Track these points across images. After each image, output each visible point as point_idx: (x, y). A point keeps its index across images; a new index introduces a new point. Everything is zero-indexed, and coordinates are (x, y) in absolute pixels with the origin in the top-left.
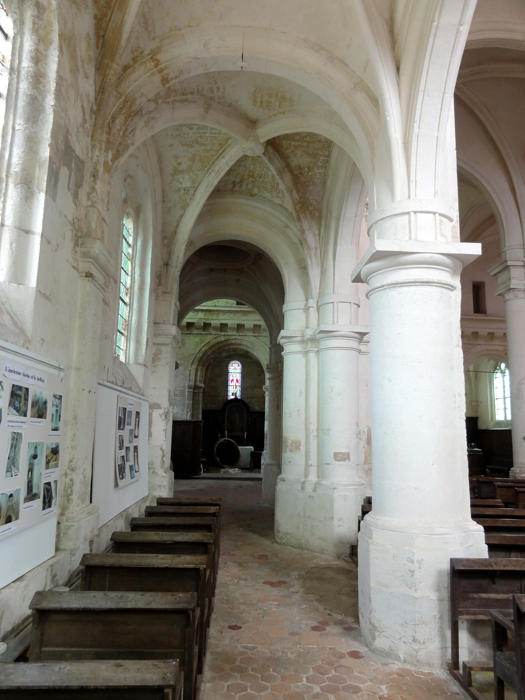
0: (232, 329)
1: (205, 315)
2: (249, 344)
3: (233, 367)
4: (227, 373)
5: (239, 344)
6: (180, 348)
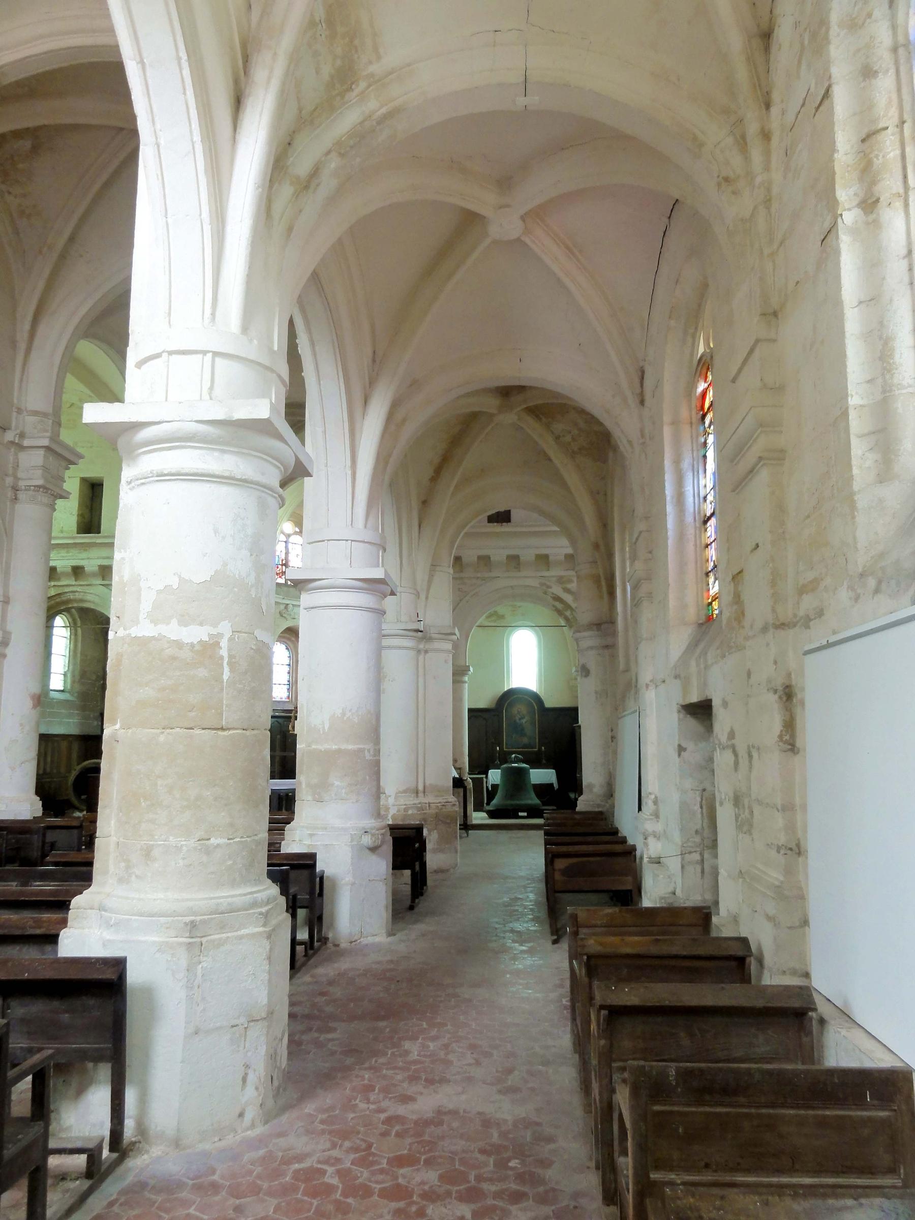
2: (96, 599)
5: (82, 601)
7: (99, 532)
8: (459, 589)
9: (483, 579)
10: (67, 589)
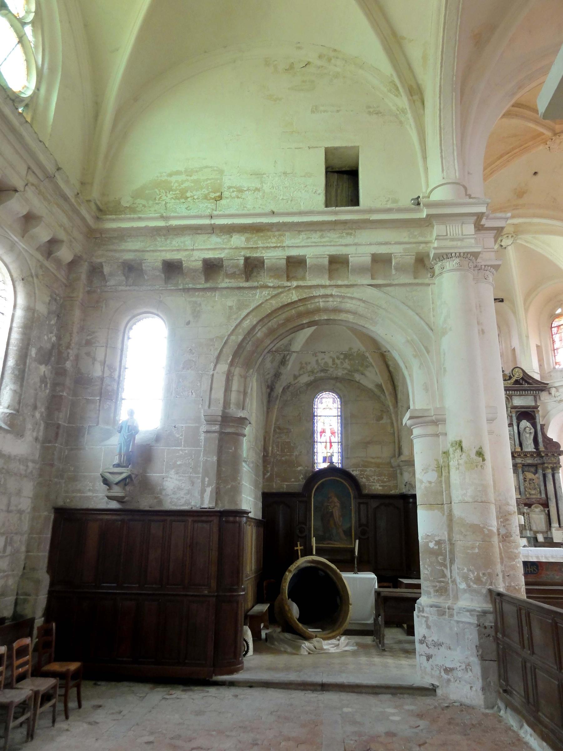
0: (318, 269)
1: (247, 240)
2: (361, 309)
3: (324, 405)
4: (311, 417)
6: (188, 323)
10: (316, 293)
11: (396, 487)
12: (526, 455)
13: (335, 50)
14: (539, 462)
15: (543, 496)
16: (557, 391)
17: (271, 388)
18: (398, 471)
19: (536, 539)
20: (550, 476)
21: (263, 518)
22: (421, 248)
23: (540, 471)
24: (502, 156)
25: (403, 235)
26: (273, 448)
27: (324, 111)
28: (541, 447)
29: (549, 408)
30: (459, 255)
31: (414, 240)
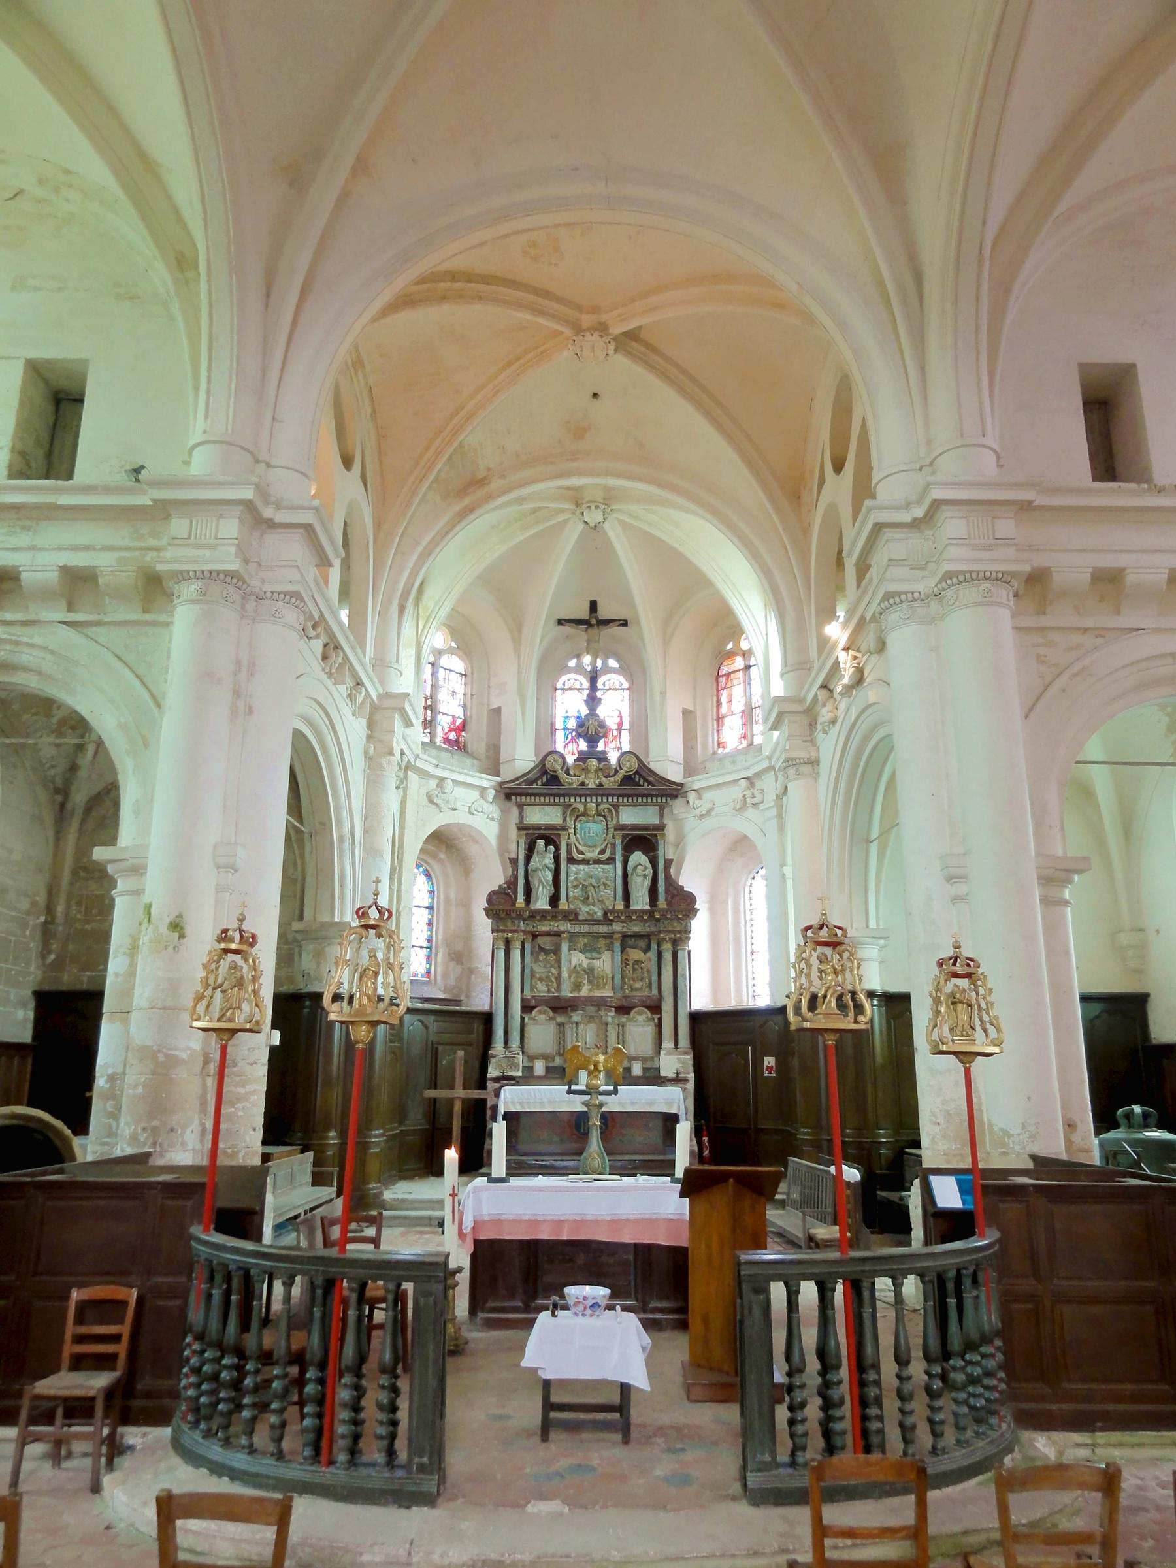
7: (70, 476)
8: (1040, 659)
9: (1099, 632)
11: (291, 980)
12: (628, 914)
13: (67, 172)
14: (653, 929)
15: (655, 992)
16: (700, 798)
17: (62, 792)
18: (297, 950)
19: (628, 1070)
20: (668, 957)
21: (35, 1038)
22: (148, 558)
23: (654, 946)
24: (509, 364)
25: (119, 535)
26: (68, 907)
27: (37, 289)
28: (662, 903)
29: (686, 829)
30: (202, 575)
31: (137, 544)
